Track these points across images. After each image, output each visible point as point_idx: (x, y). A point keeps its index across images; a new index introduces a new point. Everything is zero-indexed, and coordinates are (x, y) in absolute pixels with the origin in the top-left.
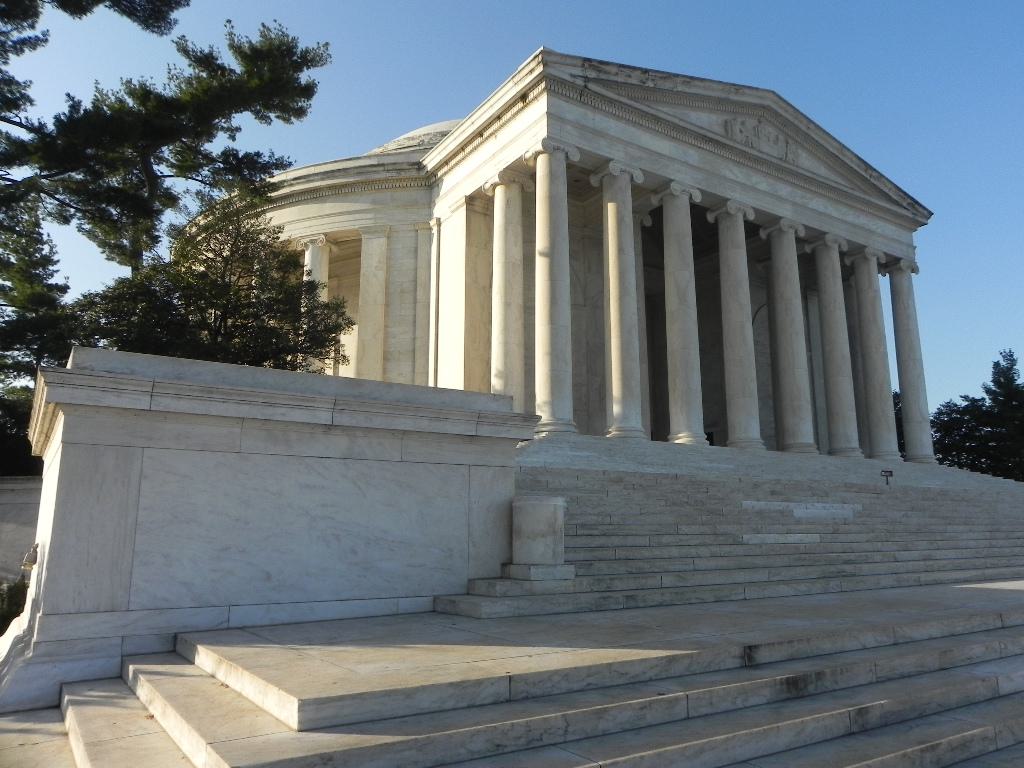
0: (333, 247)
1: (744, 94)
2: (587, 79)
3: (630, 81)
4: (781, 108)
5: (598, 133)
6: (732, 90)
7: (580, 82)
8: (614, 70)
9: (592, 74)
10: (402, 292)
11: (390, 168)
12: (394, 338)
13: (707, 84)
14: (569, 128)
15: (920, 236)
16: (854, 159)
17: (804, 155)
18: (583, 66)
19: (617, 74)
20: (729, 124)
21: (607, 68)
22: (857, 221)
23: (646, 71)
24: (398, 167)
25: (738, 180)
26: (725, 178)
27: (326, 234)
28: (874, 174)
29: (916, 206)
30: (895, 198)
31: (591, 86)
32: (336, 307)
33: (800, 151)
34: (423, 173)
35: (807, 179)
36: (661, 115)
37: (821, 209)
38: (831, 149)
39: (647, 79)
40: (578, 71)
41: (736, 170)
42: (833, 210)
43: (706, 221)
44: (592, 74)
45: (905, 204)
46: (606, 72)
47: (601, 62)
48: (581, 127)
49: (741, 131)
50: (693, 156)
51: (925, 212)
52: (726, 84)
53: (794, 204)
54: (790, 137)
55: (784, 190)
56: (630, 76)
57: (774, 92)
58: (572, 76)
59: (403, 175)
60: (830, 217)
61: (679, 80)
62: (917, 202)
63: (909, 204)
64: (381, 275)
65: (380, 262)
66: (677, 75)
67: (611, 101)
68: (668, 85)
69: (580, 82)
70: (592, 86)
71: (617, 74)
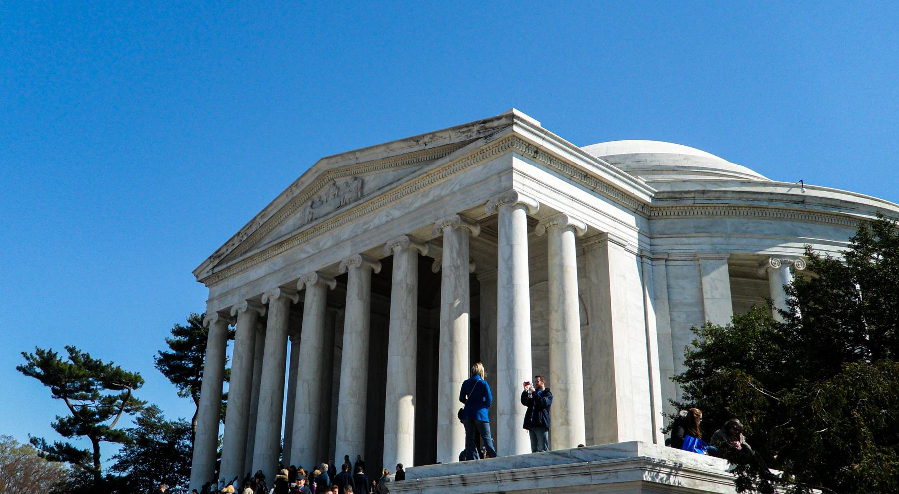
21: (221, 252)
23: (239, 233)
28: (426, 139)
29: (487, 125)
31: (216, 270)
40: (211, 266)
47: (217, 252)
52: (287, 190)
61: (257, 220)
62: (485, 122)
63: (479, 132)
66: (255, 218)
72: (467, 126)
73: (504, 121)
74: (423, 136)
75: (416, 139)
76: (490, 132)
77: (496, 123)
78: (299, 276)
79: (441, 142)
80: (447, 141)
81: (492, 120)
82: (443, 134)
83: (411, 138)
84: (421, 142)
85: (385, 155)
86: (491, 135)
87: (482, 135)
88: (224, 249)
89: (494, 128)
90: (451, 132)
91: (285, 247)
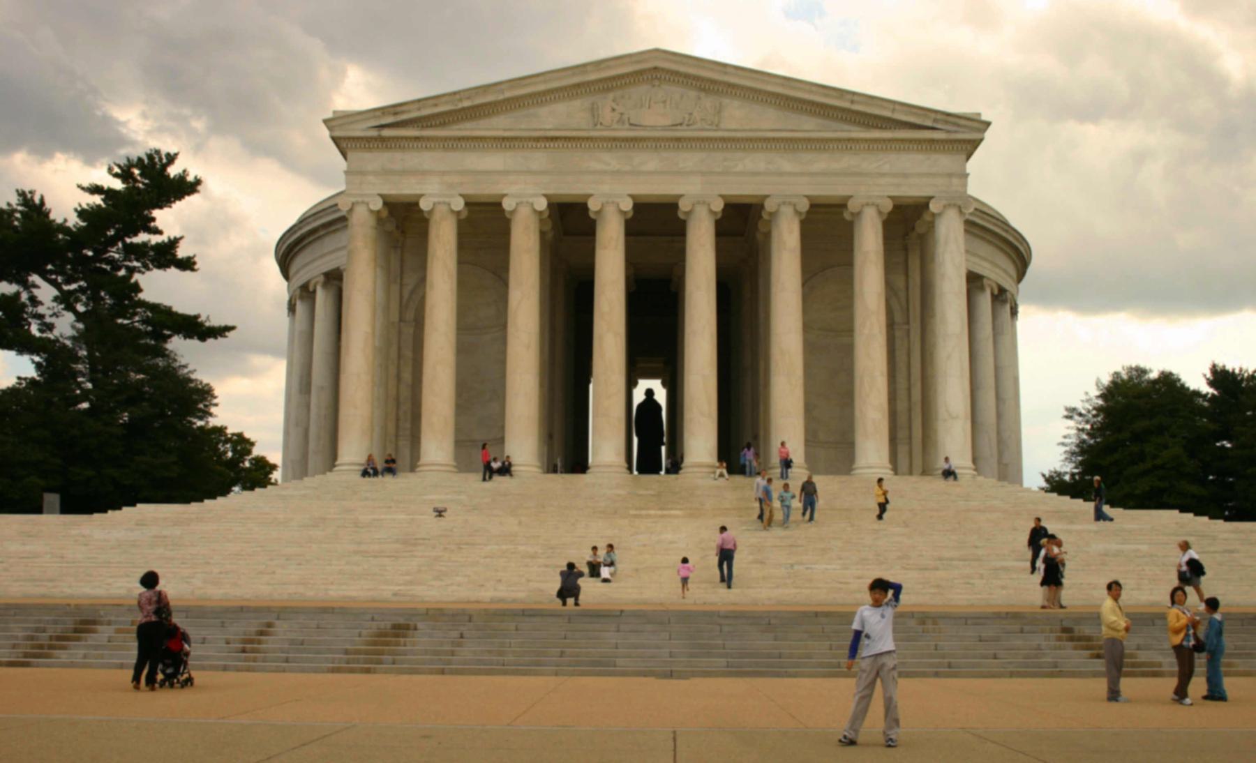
1: (609, 67)
7: (374, 133)
8: (416, 106)
14: (371, 178)
22: (835, 166)
23: (455, 93)
28: (856, 98)
33: (726, 101)
35: (723, 139)
37: (762, 166)
38: (770, 88)
39: (461, 100)
41: (606, 156)
42: (785, 163)
45: (929, 123)
46: (403, 112)
49: (614, 110)
50: (538, 159)
51: (976, 125)
53: (703, 174)
54: (704, 90)
55: (689, 160)
56: (436, 105)
60: (781, 174)
61: (503, 86)
67: (417, 138)
68: (490, 98)
70: (386, 133)
73: (976, 125)
75: (841, 93)
87: (939, 126)
89: (959, 125)
90: (897, 107)
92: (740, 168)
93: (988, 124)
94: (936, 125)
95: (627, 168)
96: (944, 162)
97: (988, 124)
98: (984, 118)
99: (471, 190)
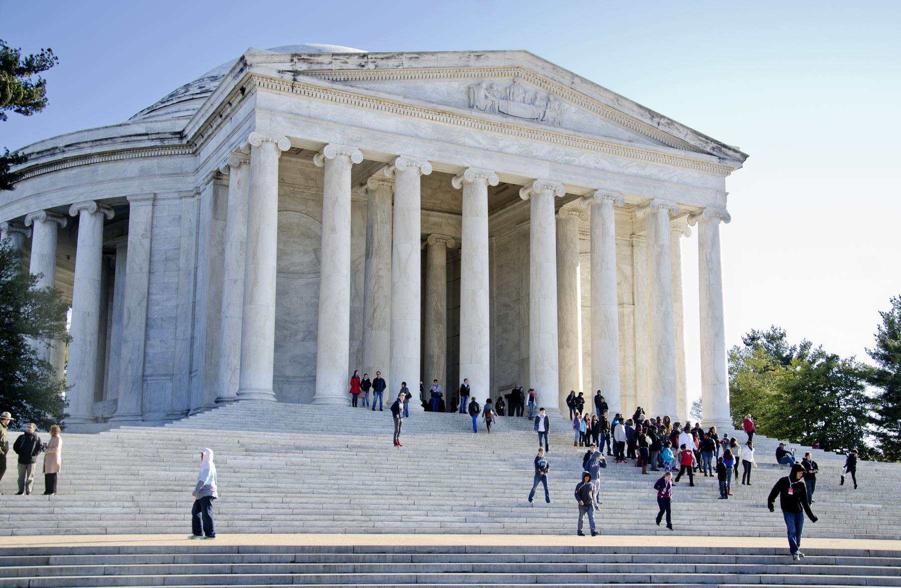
0: (107, 212)
2: (296, 73)
3: (345, 66)
4: (536, 65)
5: (311, 119)
6: (472, 57)
9: (302, 66)
10: (166, 259)
11: (154, 137)
12: (158, 305)
13: (440, 55)
14: (279, 119)
15: (735, 181)
16: (635, 108)
17: (573, 109)
18: (292, 60)
19: (331, 63)
20: (471, 90)
21: (319, 59)
22: (642, 172)
24: (161, 136)
25: (481, 146)
26: (464, 145)
27: (96, 201)
28: (662, 121)
29: (723, 149)
30: (692, 143)
31: (300, 78)
32: (54, 293)
34: (185, 142)
36: (382, 95)
37: (592, 164)
40: (288, 66)
43: (452, 187)
44: (302, 66)
45: (708, 149)
48: (294, 116)
51: (738, 155)
57: (526, 52)
58: (279, 72)
59: (166, 143)
62: (724, 146)
63: (713, 149)
64: (147, 242)
65: (146, 230)
66: (402, 54)
69: (289, 77)
71: (331, 63)
72: (707, 138)
73: (738, 155)
74: (662, 117)
75: (653, 114)
76: (722, 156)
77: (731, 153)
78: (466, 165)
79: (675, 132)
80: (682, 136)
81: (729, 148)
82: (681, 128)
83: (649, 111)
84: (657, 120)
85: (610, 104)
86: (724, 159)
87: (715, 153)
88: (326, 59)
91: (444, 117)
92: (576, 163)
93: (745, 157)
94: (712, 152)
95: (496, 149)
96: (712, 180)
97: (745, 157)
98: (742, 150)
99: (369, 147)
